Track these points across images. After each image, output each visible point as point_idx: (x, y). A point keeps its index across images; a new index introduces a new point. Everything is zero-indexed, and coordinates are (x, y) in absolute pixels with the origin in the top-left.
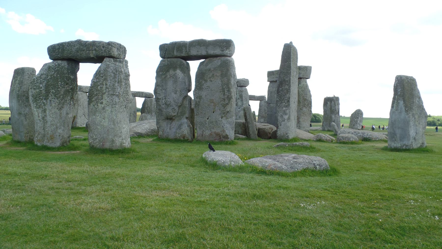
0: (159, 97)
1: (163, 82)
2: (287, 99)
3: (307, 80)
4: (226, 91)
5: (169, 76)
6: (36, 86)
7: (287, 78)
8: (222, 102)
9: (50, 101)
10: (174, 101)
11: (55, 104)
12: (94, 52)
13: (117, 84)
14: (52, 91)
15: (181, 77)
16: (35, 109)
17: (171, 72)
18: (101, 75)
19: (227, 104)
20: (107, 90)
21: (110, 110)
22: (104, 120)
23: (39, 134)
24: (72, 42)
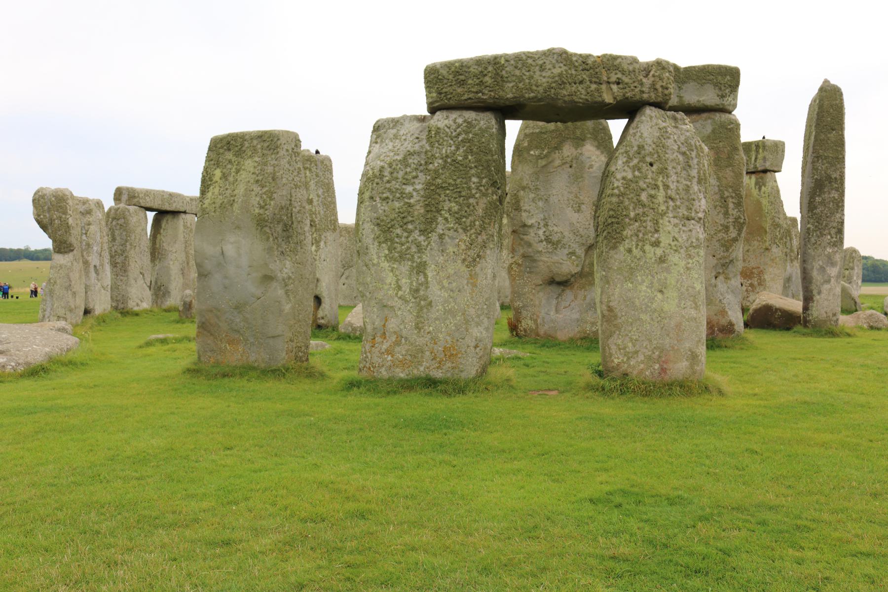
0: (529, 222)
1: (537, 179)
2: (835, 224)
3: (776, 174)
4: (731, 205)
5: (557, 162)
6: (390, 190)
7: (835, 171)
8: (721, 235)
9: (441, 237)
10: (575, 233)
11: (458, 245)
12: (615, 87)
13: (696, 188)
14: (447, 205)
15: (596, 166)
16: (386, 265)
17: (568, 150)
18: (648, 159)
19: (735, 240)
20: (671, 203)
21: (683, 263)
22: (659, 295)
23: (398, 343)
24: (529, 56)
